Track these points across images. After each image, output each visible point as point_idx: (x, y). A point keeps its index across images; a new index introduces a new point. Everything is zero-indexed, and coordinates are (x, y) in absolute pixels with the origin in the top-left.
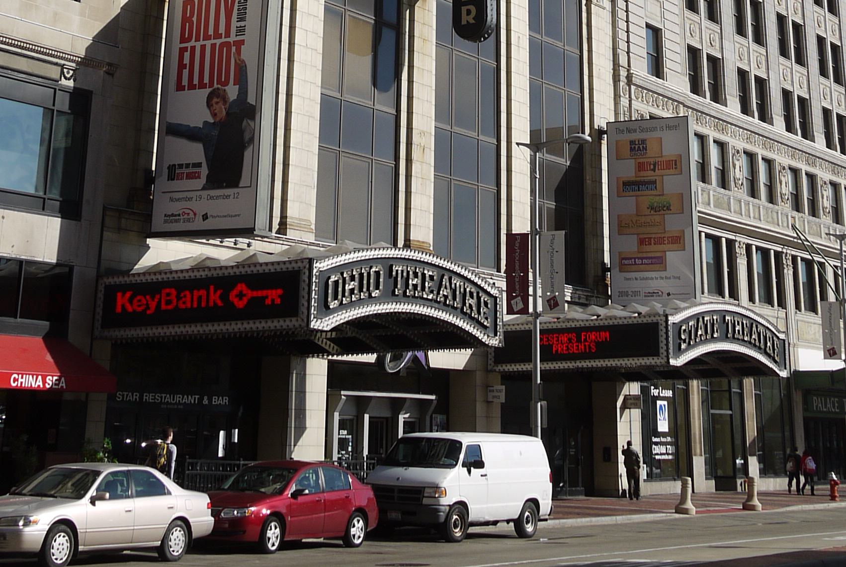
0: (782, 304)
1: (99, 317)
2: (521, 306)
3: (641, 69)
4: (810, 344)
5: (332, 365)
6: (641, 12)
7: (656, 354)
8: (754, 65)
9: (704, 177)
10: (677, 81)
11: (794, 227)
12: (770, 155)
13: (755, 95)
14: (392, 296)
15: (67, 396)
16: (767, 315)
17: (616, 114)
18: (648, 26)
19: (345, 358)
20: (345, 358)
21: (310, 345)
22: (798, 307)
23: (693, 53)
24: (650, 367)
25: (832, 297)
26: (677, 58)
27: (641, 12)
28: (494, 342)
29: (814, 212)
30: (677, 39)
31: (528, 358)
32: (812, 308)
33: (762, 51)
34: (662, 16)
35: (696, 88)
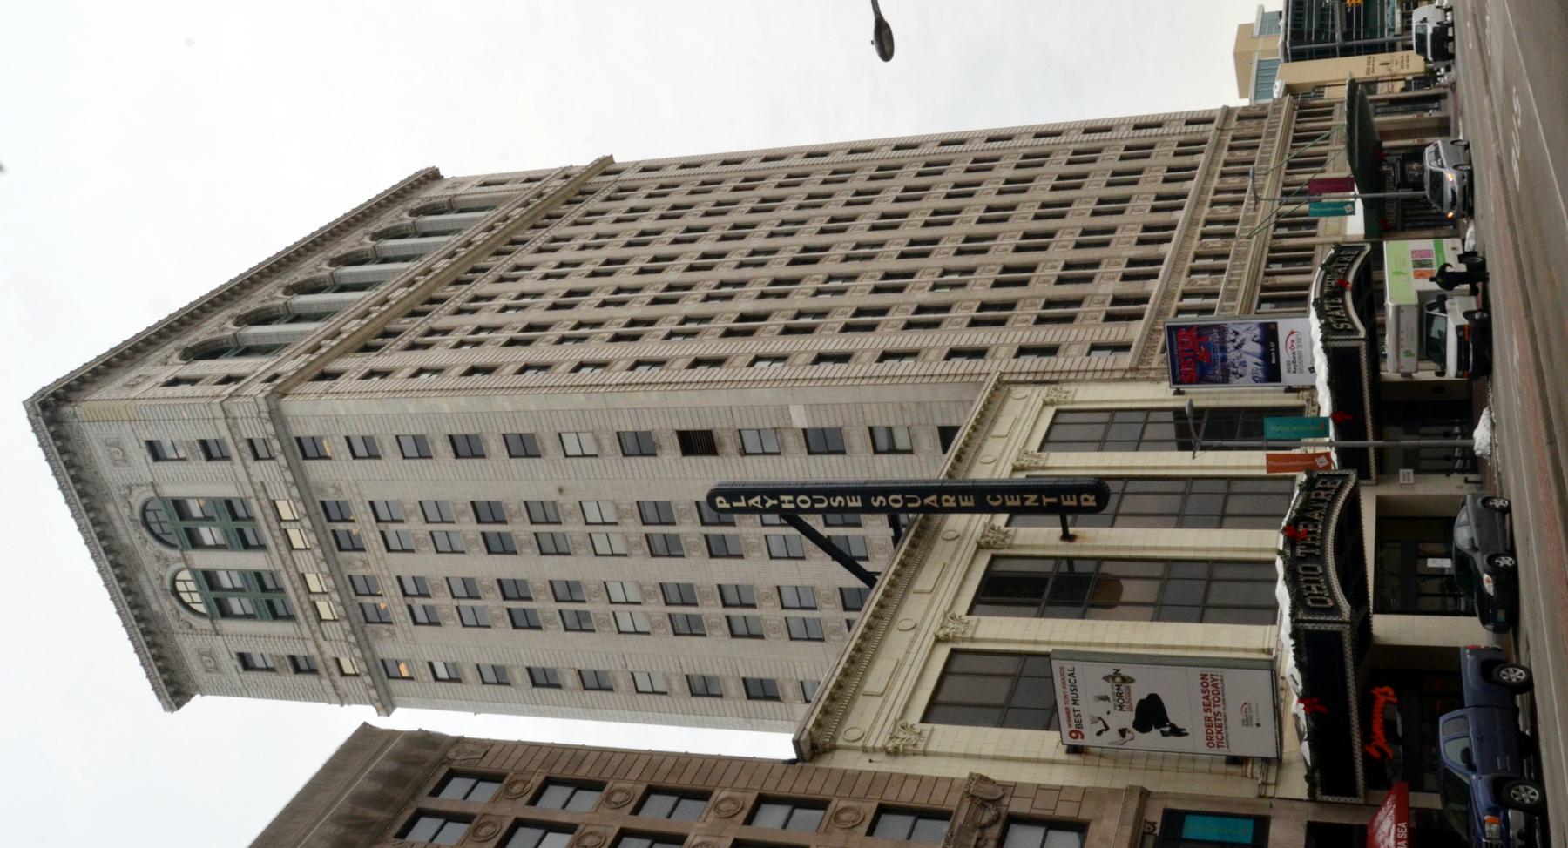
0: (1311, 248)
1: (1348, 800)
2: (1323, 458)
3: (1125, 360)
4: (1343, 225)
5: (1377, 611)
6: (1078, 360)
7: (1357, 349)
8: (1117, 269)
9: (1210, 311)
10: (1135, 332)
11: (1249, 237)
12: (1191, 256)
13: (1142, 269)
14: (1321, 559)
15: (1413, 825)
16: (1323, 255)
17: (1163, 379)
18: (1089, 354)
19: (1371, 599)
20: (1371, 599)
21: (1363, 628)
22: (1313, 235)
23: (1110, 317)
24: (1368, 356)
25: (1305, 207)
26: (1115, 331)
27: (1078, 360)
28: (1353, 476)
29: (1235, 222)
30: (1098, 331)
31: (1365, 450)
32: (1314, 224)
33: (1105, 262)
34: (1081, 342)
35: (1138, 316)
